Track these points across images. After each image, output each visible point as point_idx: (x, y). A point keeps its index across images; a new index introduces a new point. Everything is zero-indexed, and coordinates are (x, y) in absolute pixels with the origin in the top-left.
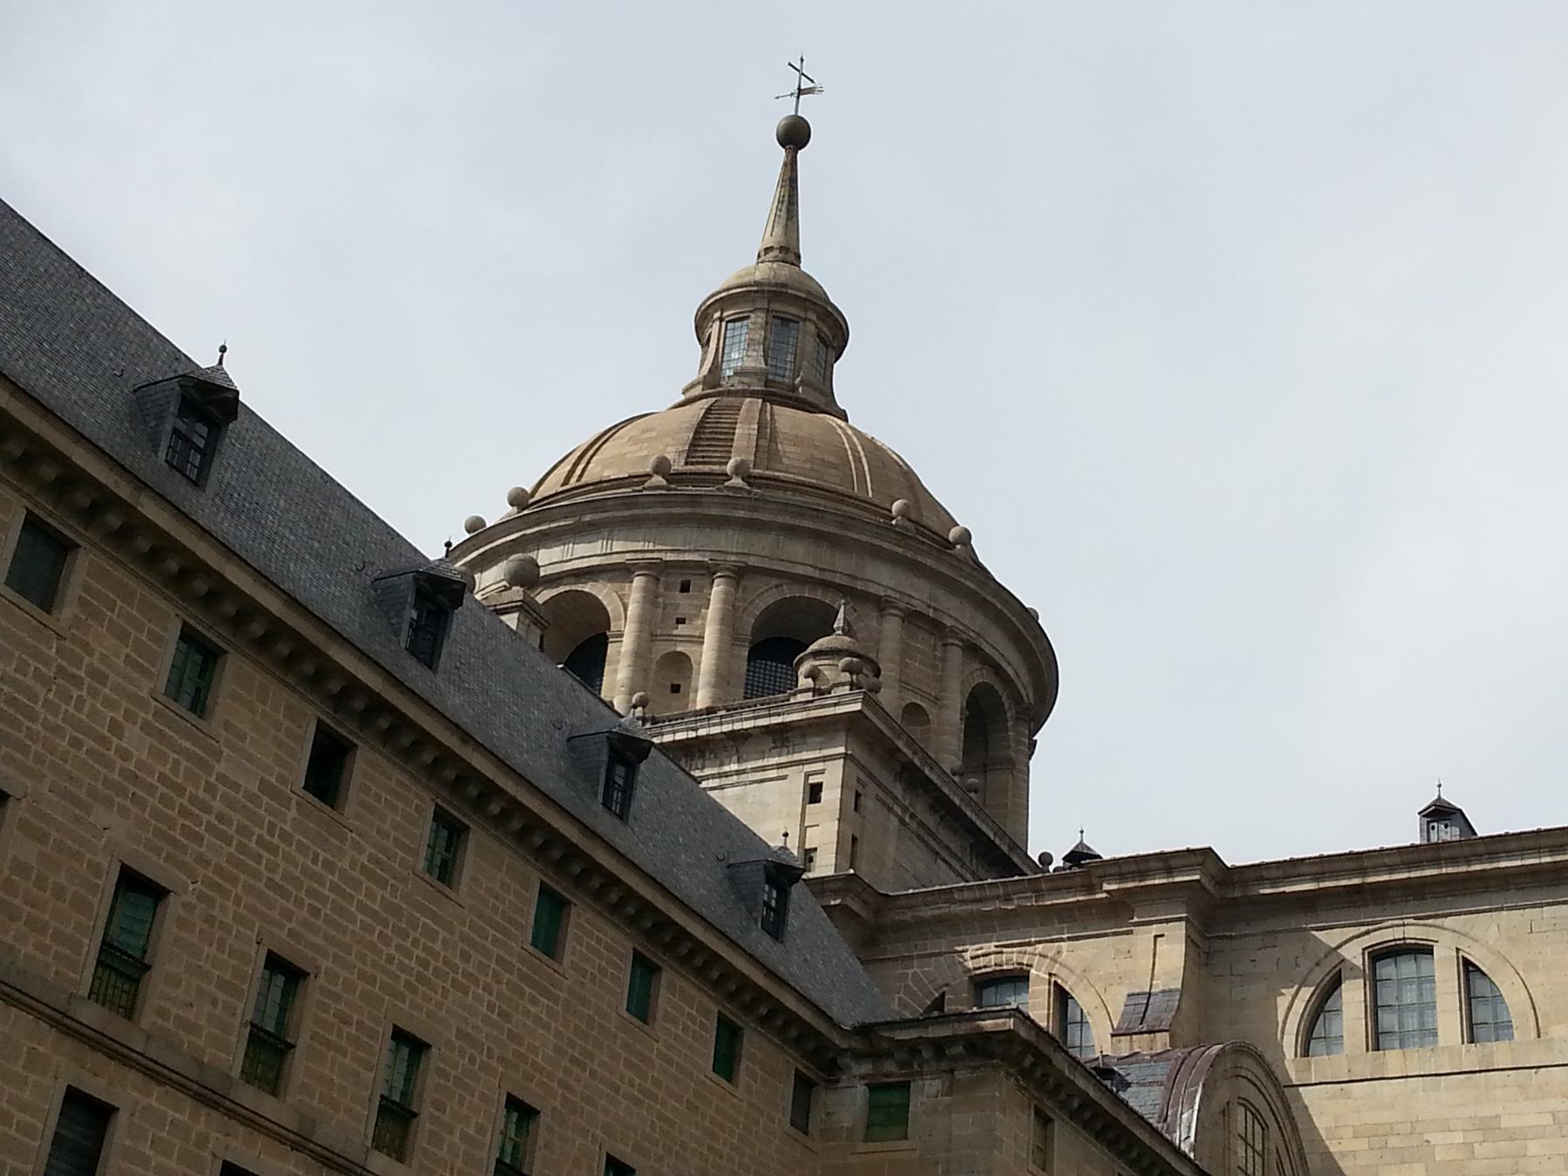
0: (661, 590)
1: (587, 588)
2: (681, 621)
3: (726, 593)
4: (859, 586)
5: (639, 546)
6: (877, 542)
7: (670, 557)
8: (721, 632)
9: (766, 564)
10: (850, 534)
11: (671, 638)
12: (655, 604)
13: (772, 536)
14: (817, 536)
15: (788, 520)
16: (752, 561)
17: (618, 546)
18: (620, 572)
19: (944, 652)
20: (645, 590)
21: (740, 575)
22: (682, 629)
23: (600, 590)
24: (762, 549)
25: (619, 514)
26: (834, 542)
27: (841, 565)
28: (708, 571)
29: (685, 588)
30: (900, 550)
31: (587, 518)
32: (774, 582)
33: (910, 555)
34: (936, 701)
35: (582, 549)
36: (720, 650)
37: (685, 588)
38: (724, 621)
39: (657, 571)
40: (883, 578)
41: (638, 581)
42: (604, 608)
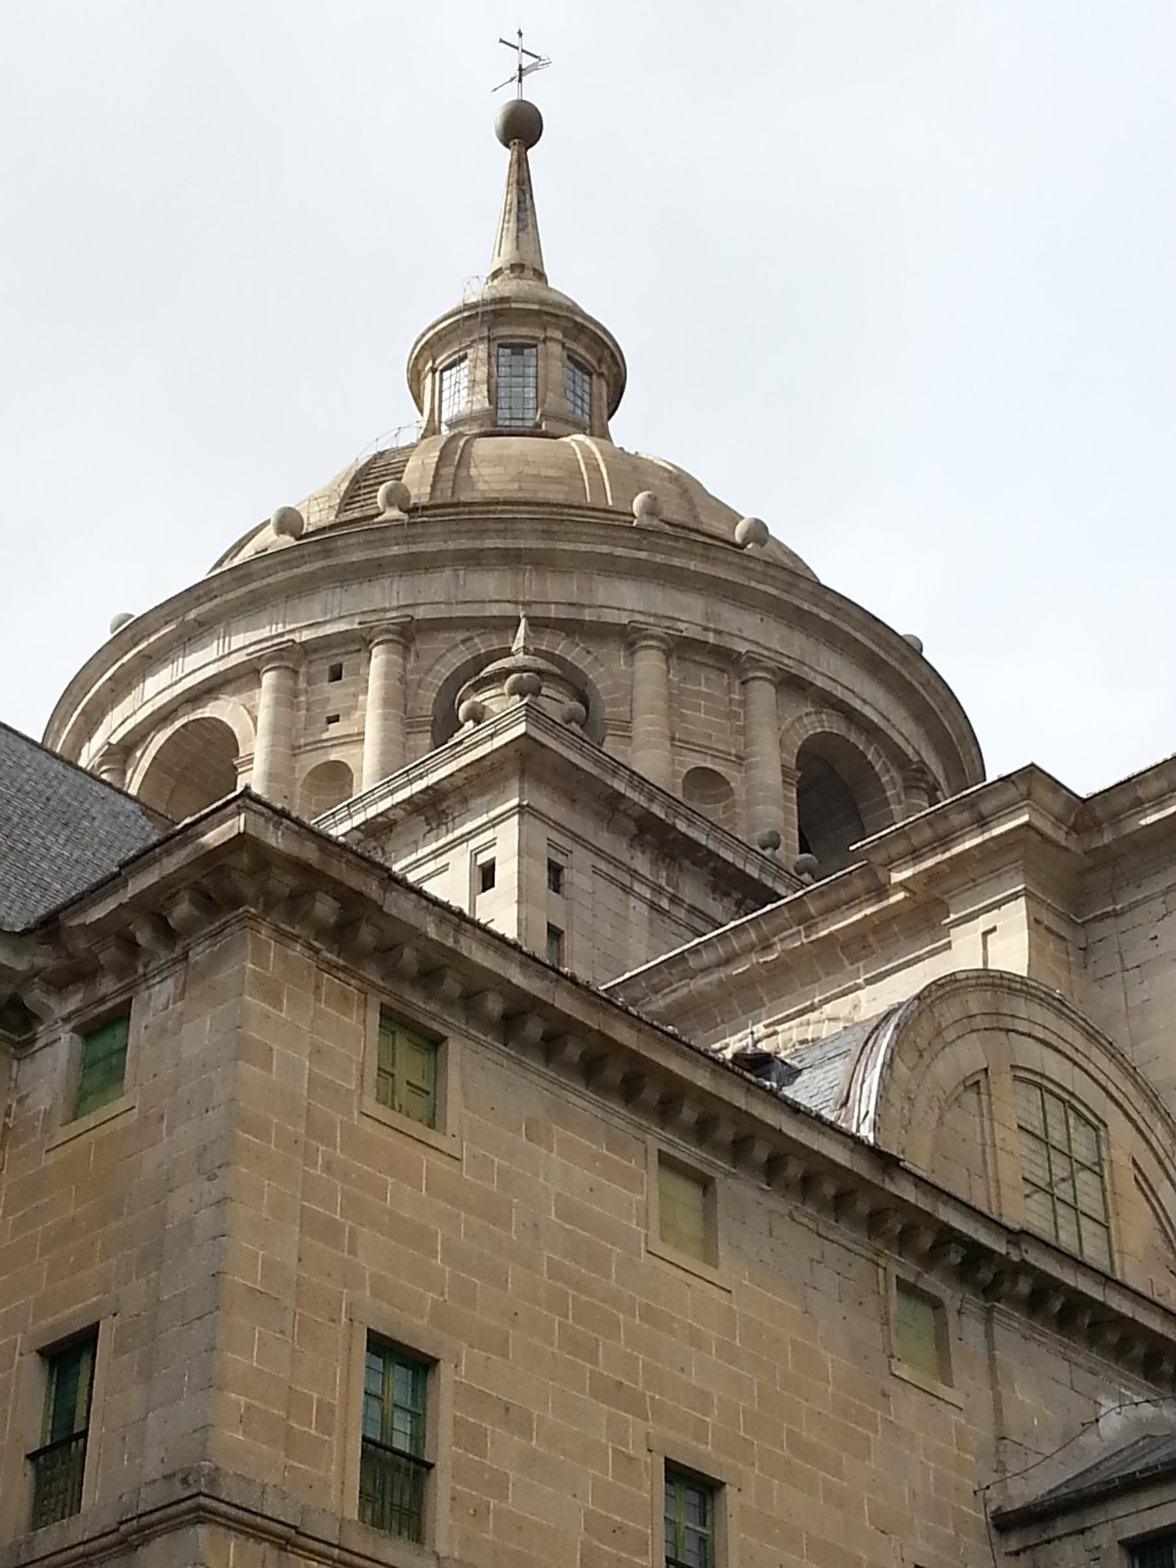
0: (302, 685)
1: (208, 711)
2: (336, 719)
3: (388, 663)
4: (587, 615)
5: (265, 632)
6: (605, 549)
7: (306, 635)
8: (385, 718)
9: (443, 612)
10: (561, 546)
11: (319, 745)
12: (293, 706)
13: (448, 572)
14: (511, 559)
15: (465, 544)
16: (420, 613)
17: (238, 641)
18: (243, 677)
19: (745, 693)
20: (277, 689)
21: (407, 635)
22: (335, 730)
23: (223, 709)
24: (432, 594)
25: (230, 596)
26: (541, 562)
27: (557, 593)
28: (360, 642)
29: (336, 675)
30: (643, 555)
31: (192, 615)
32: (461, 636)
33: (659, 558)
34: (740, 760)
35: (194, 659)
36: (386, 742)
37: (336, 675)
38: (387, 702)
39: (292, 658)
40: (623, 600)
41: (268, 679)
42: (232, 733)
